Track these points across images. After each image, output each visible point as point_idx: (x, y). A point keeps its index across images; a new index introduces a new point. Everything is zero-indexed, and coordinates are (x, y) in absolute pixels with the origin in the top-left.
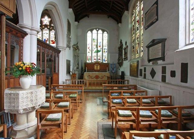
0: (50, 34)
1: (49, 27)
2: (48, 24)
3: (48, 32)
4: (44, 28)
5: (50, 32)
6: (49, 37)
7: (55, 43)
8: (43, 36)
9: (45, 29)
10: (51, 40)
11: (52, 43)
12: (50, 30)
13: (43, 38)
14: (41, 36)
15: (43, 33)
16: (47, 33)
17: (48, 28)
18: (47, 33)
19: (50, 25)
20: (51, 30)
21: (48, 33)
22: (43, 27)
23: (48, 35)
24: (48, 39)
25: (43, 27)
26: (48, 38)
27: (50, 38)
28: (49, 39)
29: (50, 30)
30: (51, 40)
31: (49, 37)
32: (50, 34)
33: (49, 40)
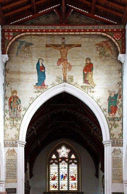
0: (68, 168)
1: (67, 160)
2: (66, 156)
3: (66, 166)
4: (61, 162)
5: (68, 166)
6: (68, 172)
7: (76, 179)
8: (60, 171)
9: (62, 162)
10: (71, 176)
11: (72, 180)
12: (69, 164)
13: (60, 173)
14: (57, 171)
15: (60, 167)
16: (65, 168)
17: (66, 162)
18: (65, 168)
19: (69, 158)
20: (71, 163)
21: (67, 167)
22: (60, 160)
23: (67, 169)
24: (66, 175)
25: (60, 160)
26: (67, 173)
27: (70, 173)
28: (68, 174)
29: (69, 164)
30: (71, 176)
31: (68, 172)
32: (68, 168)
33: (68, 176)
